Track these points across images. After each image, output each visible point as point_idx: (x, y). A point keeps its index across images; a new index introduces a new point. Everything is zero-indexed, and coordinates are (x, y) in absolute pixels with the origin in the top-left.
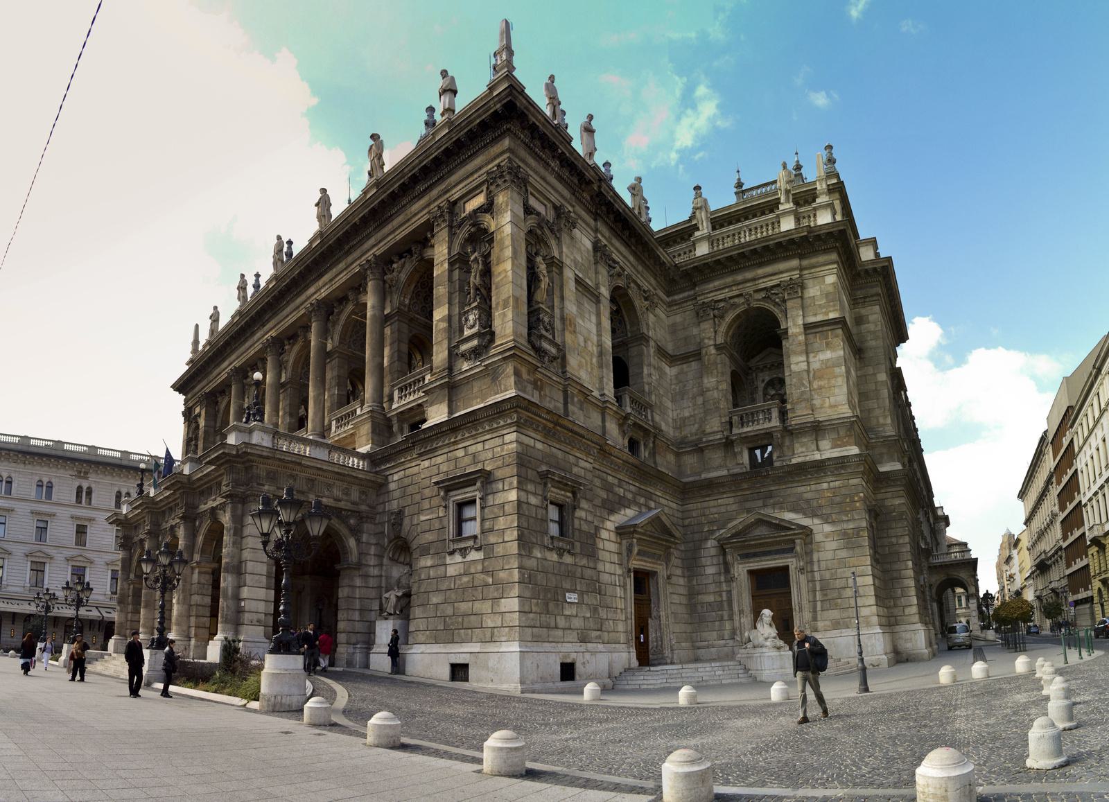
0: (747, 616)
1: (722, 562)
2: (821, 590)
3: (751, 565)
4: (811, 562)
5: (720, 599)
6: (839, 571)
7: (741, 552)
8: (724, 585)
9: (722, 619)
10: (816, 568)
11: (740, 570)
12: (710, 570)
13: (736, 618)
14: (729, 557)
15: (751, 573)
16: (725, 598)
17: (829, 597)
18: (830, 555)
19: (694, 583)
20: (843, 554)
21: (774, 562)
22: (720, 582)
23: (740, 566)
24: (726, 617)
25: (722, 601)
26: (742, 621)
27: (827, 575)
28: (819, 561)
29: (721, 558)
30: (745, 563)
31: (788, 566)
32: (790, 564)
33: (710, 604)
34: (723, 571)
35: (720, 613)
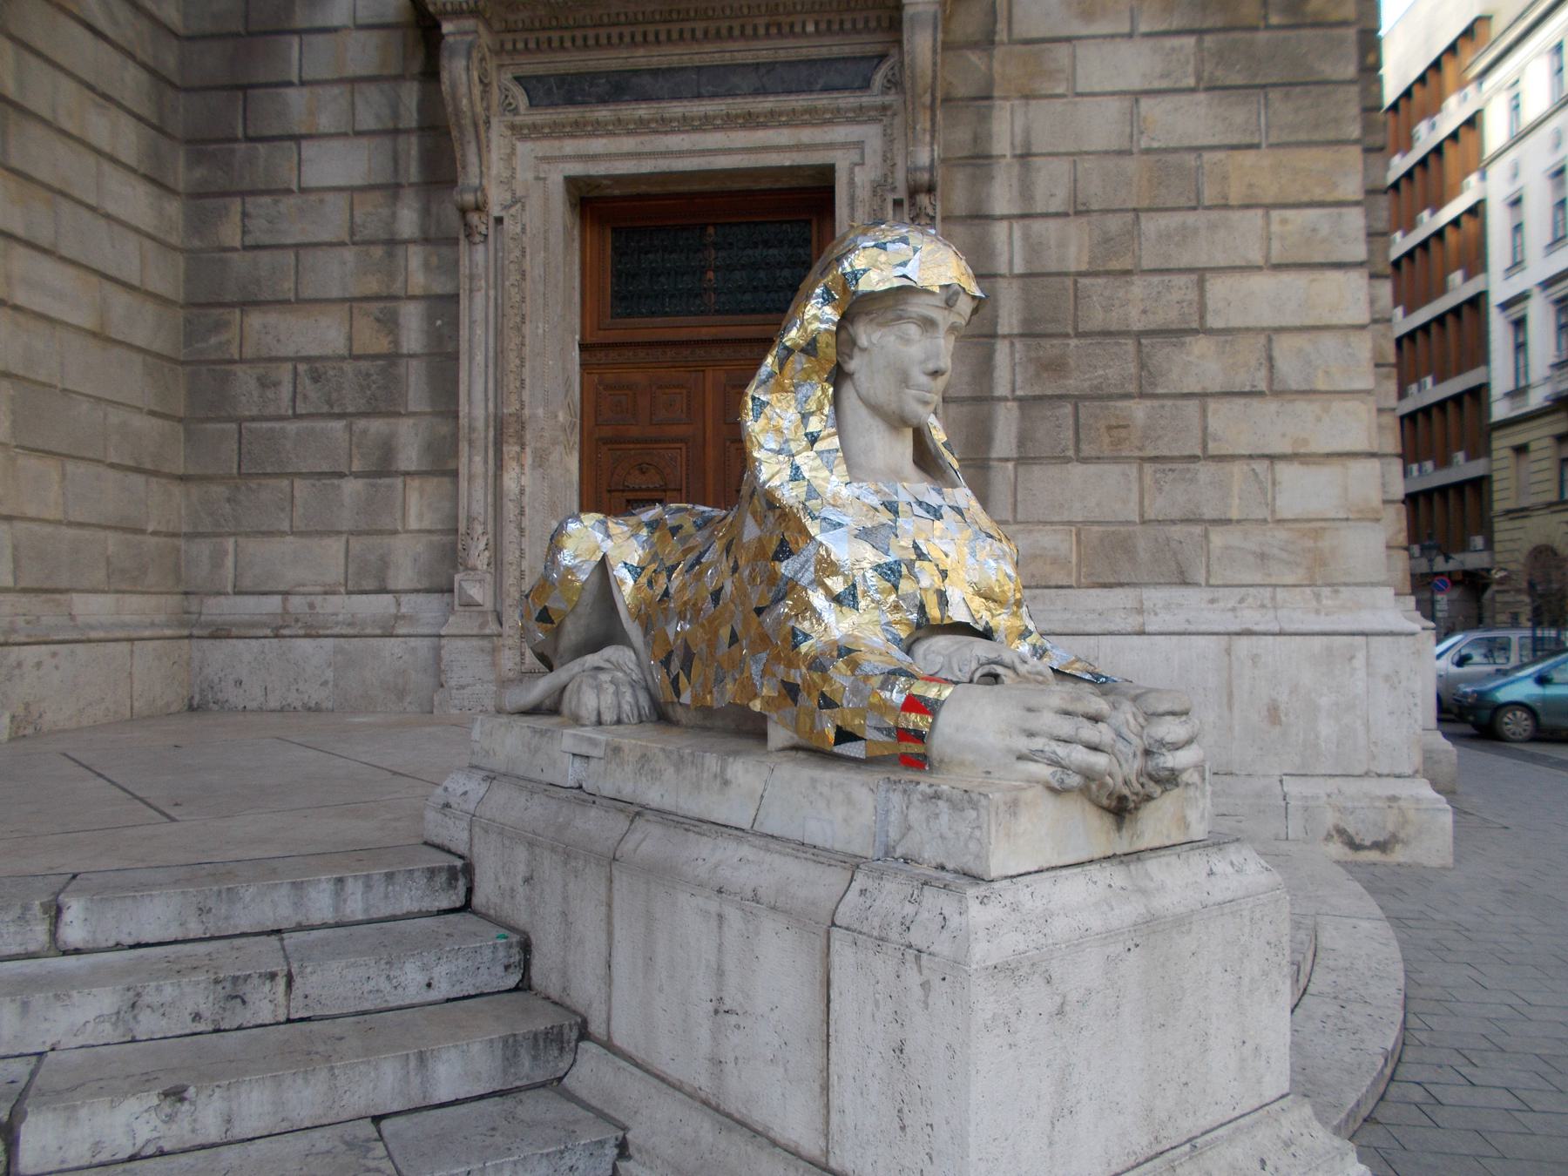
0: (541, 460)
1: (410, 118)
2: (1031, 333)
3: (598, 145)
4: (979, 160)
5: (382, 345)
6: (1151, 225)
7: (535, 65)
8: (415, 258)
9: (383, 467)
10: (1002, 198)
11: (524, 175)
12: (336, 165)
13: (474, 463)
14: (457, 71)
15: (593, 203)
16: (413, 337)
17: (1073, 384)
18: (1100, 125)
19: (230, 233)
20: (1187, 121)
21: (741, 138)
22: (392, 243)
23: (524, 148)
24: (410, 456)
25: (393, 358)
26: (510, 482)
27: (1071, 247)
28: (1025, 156)
29: (410, 94)
30: (556, 131)
31: (828, 172)
32: (842, 162)
33: (315, 367)
34: (413, 172)
35: (377, 426)
